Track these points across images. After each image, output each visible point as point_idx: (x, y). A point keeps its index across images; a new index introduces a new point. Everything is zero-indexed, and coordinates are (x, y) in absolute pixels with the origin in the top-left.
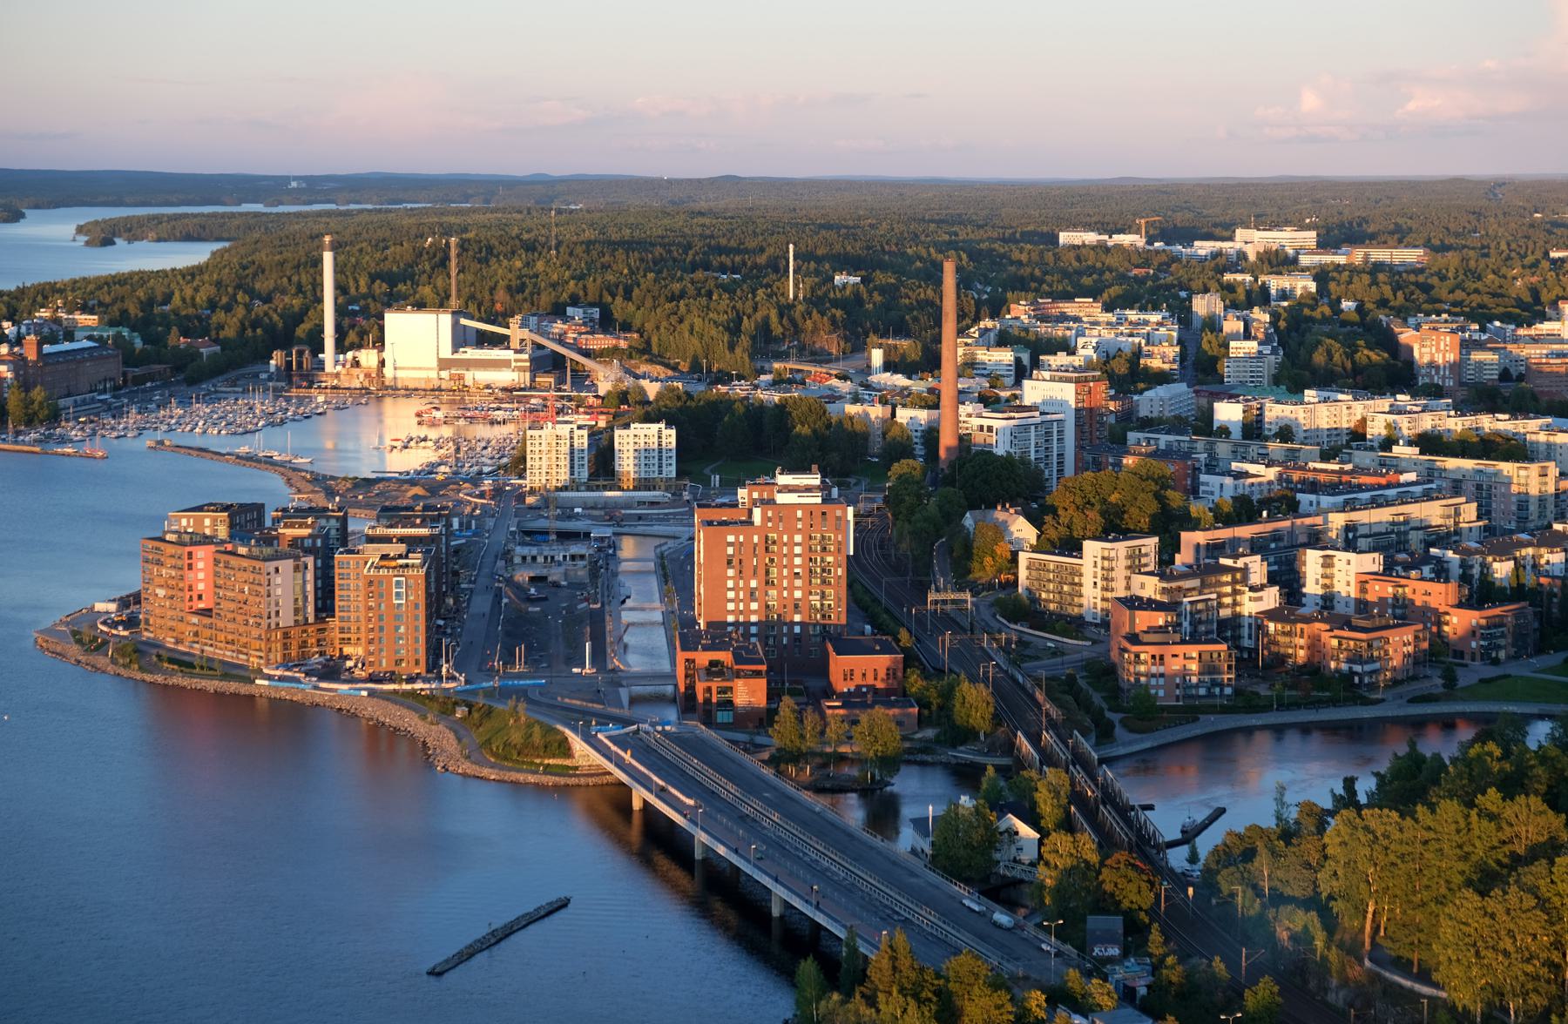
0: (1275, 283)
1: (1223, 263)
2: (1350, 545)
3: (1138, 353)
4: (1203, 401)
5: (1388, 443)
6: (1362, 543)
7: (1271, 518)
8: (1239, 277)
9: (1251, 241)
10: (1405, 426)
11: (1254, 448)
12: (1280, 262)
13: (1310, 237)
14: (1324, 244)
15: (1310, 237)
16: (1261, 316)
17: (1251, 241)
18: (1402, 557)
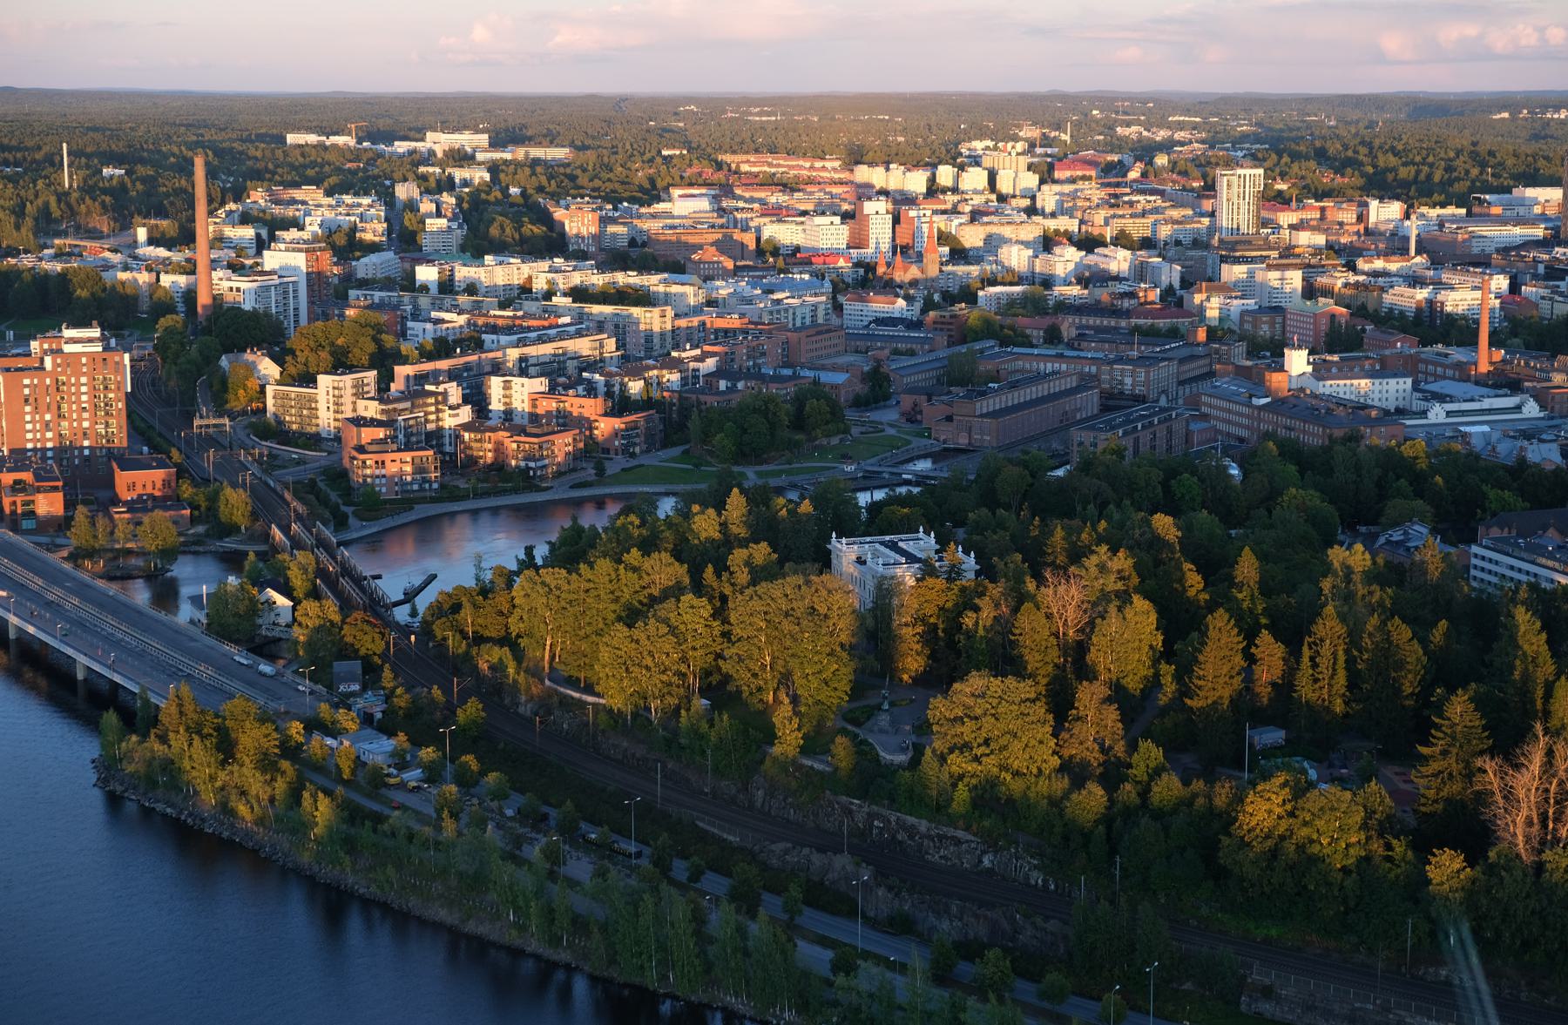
0: (459, 174)
1: (416, 159)
2: (523, 373)
3: (354, 229)
4: (407, 265)
5: (548, 295)
6: (532, 370)
7: (463, 353)
8: (431, 169)
9: (438, 142)
10: (562, 283)
11: (448, 301)
12: (462, 158)
13: (483, 139)
14: (495, 144)
15: (483, 139)
16: (448, 199)
17: (438, 142)
18: (562, 380)
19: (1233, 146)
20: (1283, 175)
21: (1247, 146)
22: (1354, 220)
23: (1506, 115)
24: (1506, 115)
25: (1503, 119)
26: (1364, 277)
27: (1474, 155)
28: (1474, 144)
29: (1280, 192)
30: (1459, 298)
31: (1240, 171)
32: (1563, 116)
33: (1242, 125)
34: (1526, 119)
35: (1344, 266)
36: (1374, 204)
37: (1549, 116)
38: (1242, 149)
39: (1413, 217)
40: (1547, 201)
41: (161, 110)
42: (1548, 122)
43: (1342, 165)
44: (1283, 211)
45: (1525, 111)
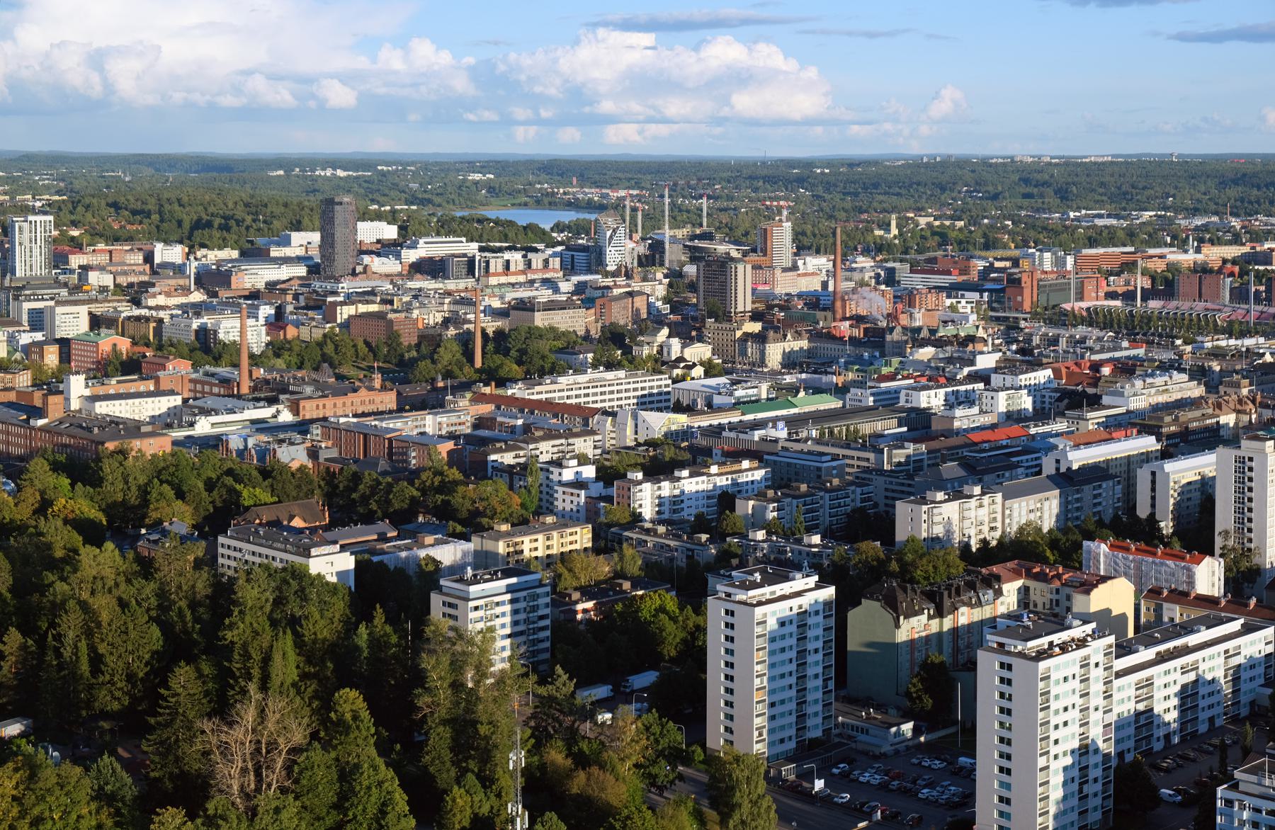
19: (34, 198)
20: (75, 224)
21: (47, 197)
22: (141, 261)
23: (281, 172)
24: (281, 172)
25: (280, 176)
26: (146, 311)
27: (247, 205)
28: (252, 197)
29: (73, 238)
30: (230, 326)
31: (31, 218)
32: (328, 174)
33: (44, 180)
34: (298, 176)
35: (128, 301)
36: (159, 247)
37: (317, 173)
38: (40, 200)
39: (192, 258)
40: (309, 243)
41: (147, 186)
42: (315, 179)
43: (140, 213)
44: (74, 253)
45: (298, 170)
